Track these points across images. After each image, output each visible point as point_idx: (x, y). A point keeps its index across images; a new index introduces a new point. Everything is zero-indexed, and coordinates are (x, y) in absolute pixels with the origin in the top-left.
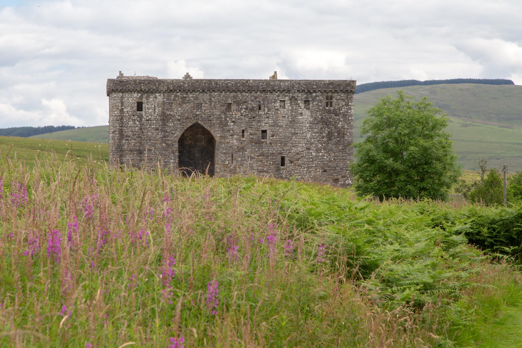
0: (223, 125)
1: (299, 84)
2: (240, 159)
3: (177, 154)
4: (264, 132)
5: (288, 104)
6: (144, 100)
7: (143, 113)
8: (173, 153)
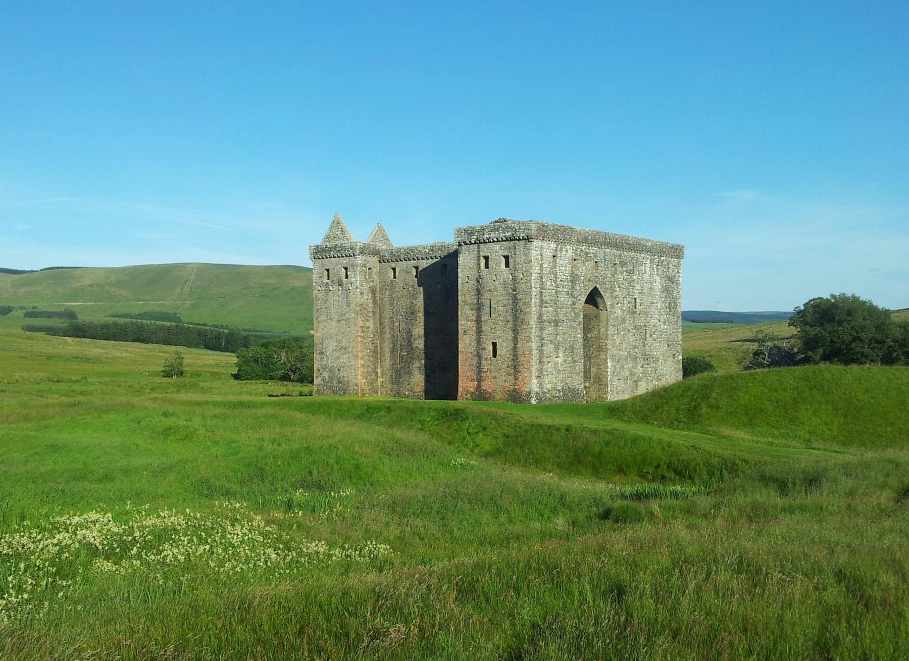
0: (612, 289)
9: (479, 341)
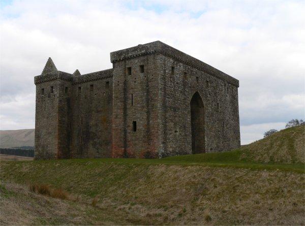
9: (125, 120)
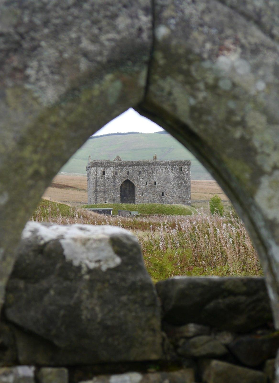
0: (138, 180)
1: (169, 162)
2: (145, 194)
3: (120, 192)
4: (155, 183)
5: (164, 171)
6: (106, 170)
7: (105, 175)
8: (118, 192)
